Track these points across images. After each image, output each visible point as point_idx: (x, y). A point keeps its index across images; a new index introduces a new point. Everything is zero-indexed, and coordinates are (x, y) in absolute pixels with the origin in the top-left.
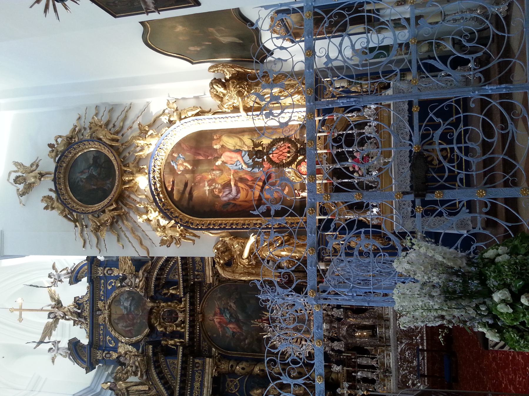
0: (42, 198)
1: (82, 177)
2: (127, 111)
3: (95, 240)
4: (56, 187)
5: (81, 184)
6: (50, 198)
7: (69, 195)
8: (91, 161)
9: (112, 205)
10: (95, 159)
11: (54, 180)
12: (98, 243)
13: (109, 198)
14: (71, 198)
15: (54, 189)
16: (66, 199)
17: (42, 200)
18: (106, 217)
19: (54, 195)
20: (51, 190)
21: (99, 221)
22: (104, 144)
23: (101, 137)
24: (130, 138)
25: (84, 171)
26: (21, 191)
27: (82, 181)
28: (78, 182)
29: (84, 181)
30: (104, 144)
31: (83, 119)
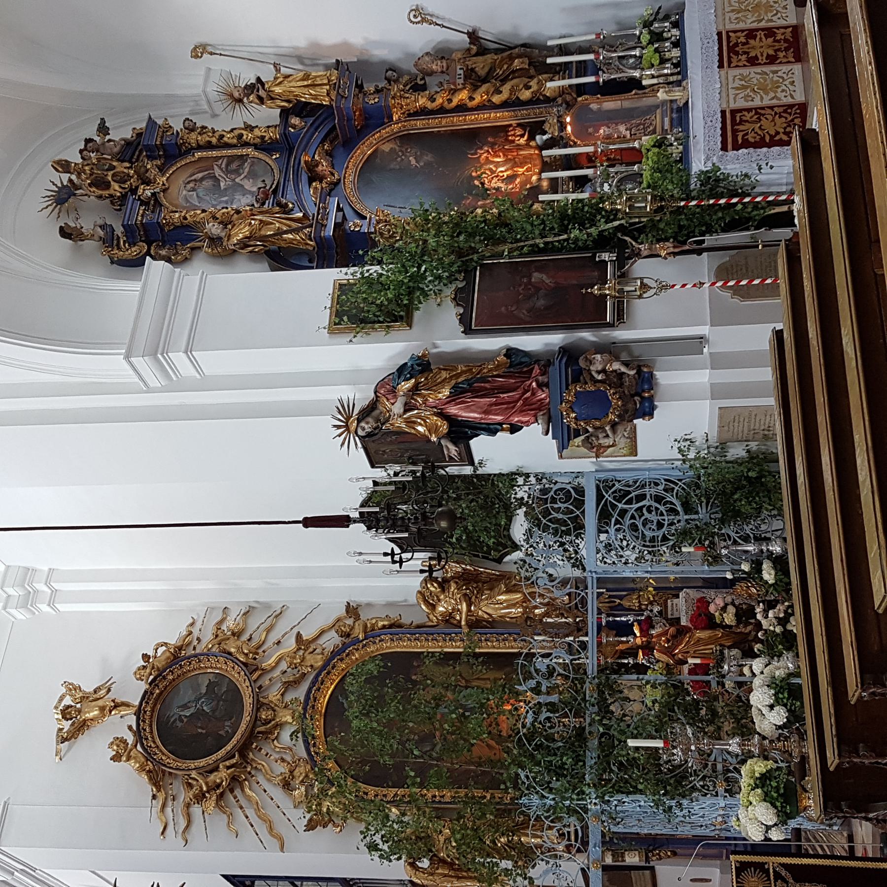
0: (112, 740)
1: (182, 713)
2: (276, 617)
3: (183, 824)
4: (138, 725)
5: (179, 724)
6: (125, 742)
7: (154, 742)
8: (204, 691)
9: (234, 756)
10: (211, 685)
11: (138, 714)
12: (187, 827)
13: (229, 747)
14: (157, 747)
15: (134, 728)
16: (150, 747)
17: (112, 743)
18: (222, 775)
19: (130, 739)
20: (130, 728)
21: (207, 784)
22: (235, 661)
23: (233, 650)
24: (272, 660)
25: (189, 705)
26: (67, 732)
27: (182, 721)
28: (175, 720)
29: (185, 720)
30: (235, 661)
31: (198, 625)
